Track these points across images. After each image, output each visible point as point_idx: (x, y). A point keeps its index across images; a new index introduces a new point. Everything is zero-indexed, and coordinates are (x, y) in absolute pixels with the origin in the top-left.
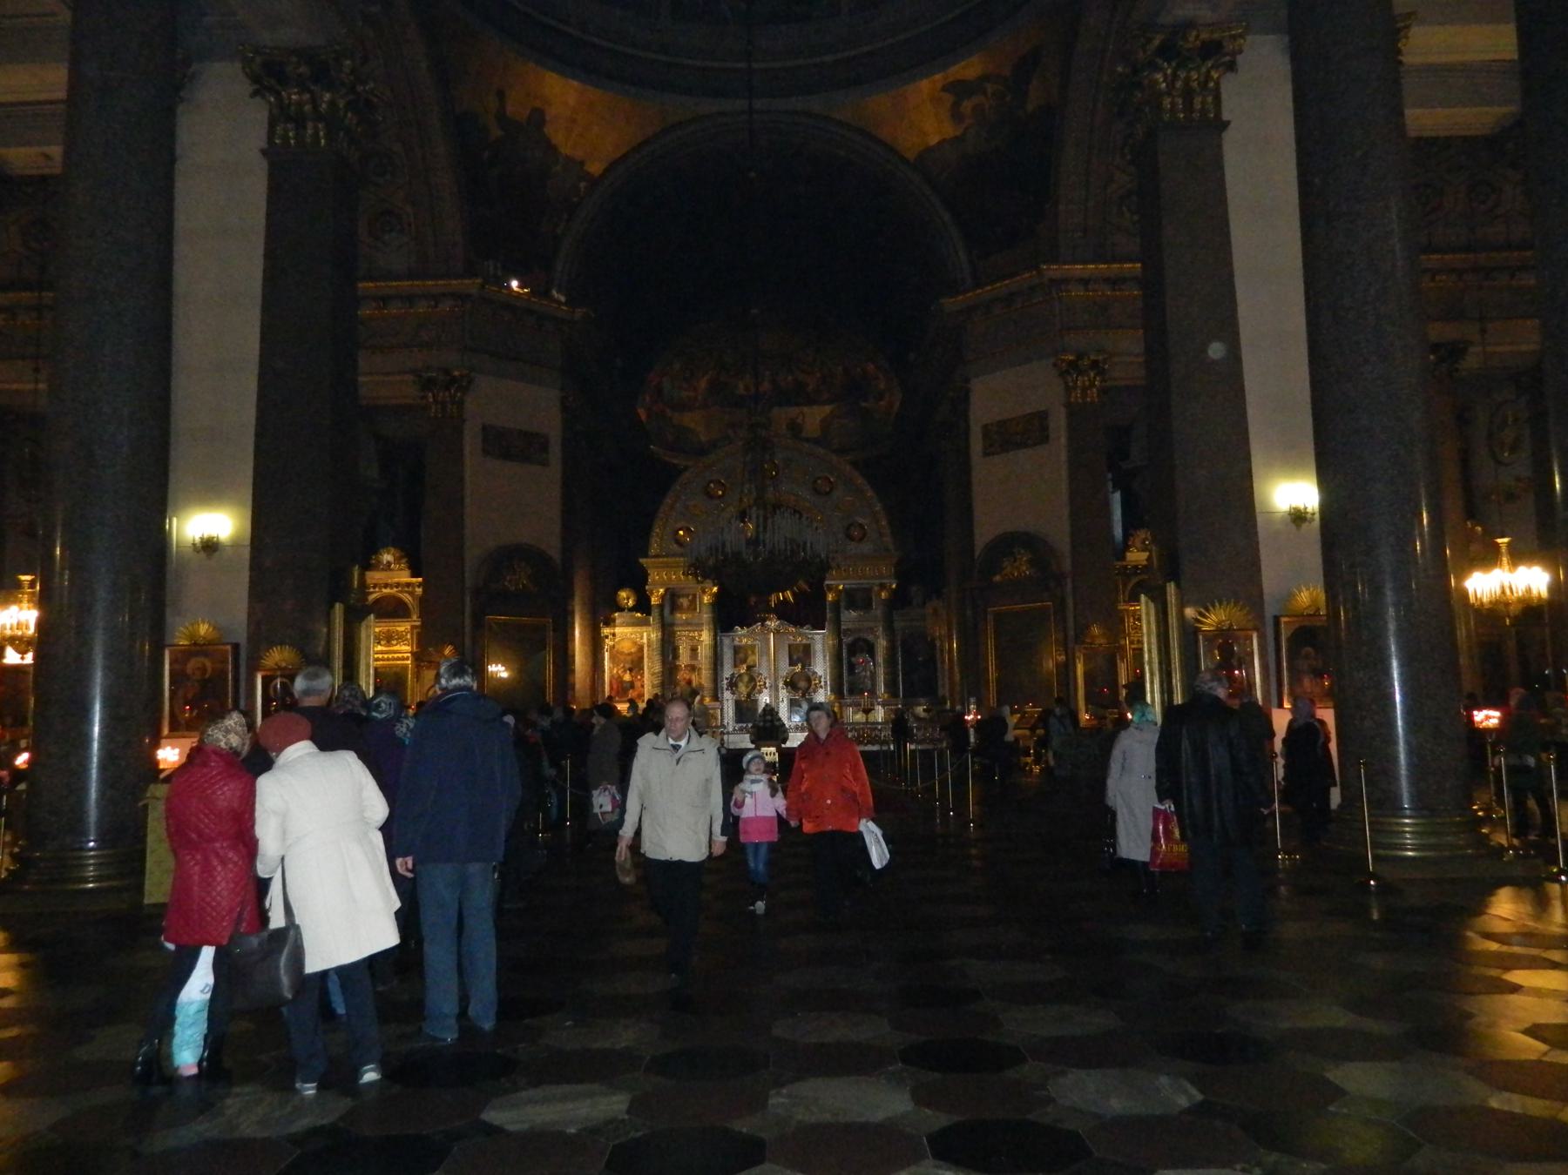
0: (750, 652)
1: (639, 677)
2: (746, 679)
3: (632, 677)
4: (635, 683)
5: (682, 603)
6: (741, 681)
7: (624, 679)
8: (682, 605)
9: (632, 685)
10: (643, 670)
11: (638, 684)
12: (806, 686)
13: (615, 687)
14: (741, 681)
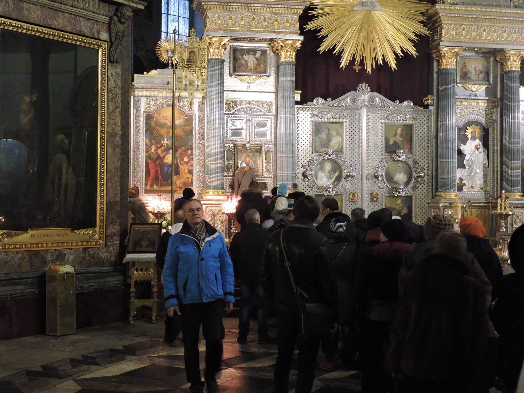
0: (334, 133)
1: (186, 159)
2: (328, 166)
6: (322, 169)
7: (165, 161)
10: (192, 149)
11: (184, 169)
14: (322, 169)
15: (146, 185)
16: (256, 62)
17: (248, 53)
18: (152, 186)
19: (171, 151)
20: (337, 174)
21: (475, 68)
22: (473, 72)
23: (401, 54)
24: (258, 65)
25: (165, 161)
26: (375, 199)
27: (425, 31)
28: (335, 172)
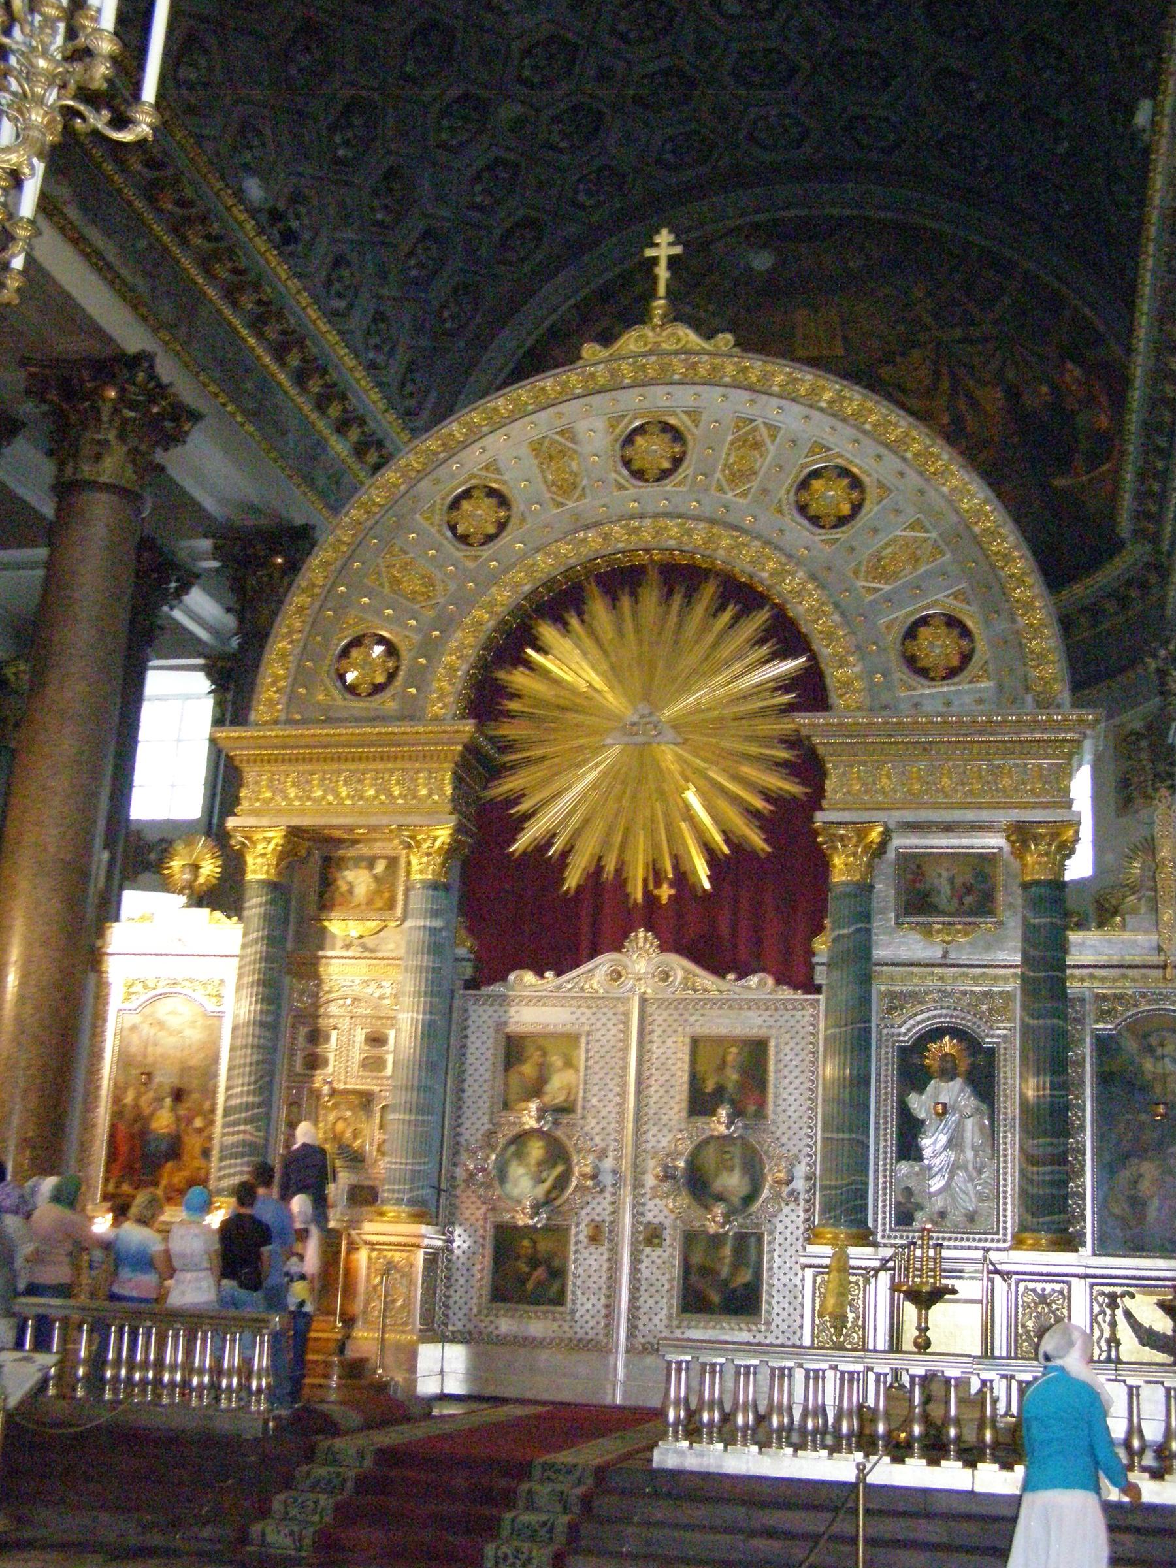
0: (556, 1060)
1: (198, 1123)
2: (536, 1150)
3: (178, 1119)
4: (186, 1139)
5: (351, 887)
6: (520, 1155)
8: (351, 891)
9: (174, 1149)
11: (193, 1143)
12: (744, 1190)
13: (124, 1149)
14: (520, 1155)
15: (106, 1180)
16: (373, 886)
17: (357, 866)
18: (118, 1185)
19: (168, 1101)
20: (560, 1169)
21: (951, 880)
22: (946, 889)
23: (726, 850)
24: (378, 892)
25: (154, 1125)
26: (656, 1241)
27: (792, 788)
28: (554, 1166)
